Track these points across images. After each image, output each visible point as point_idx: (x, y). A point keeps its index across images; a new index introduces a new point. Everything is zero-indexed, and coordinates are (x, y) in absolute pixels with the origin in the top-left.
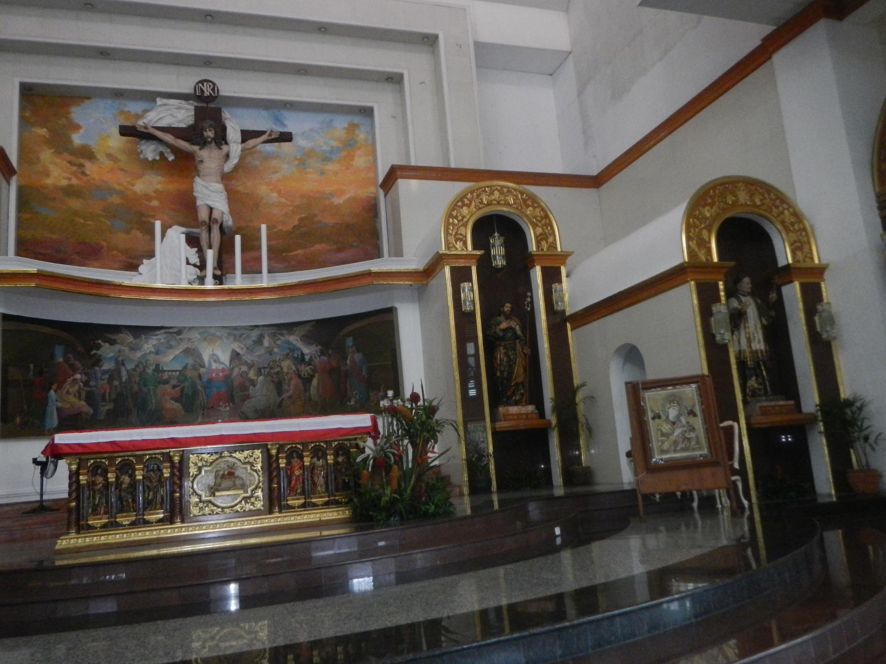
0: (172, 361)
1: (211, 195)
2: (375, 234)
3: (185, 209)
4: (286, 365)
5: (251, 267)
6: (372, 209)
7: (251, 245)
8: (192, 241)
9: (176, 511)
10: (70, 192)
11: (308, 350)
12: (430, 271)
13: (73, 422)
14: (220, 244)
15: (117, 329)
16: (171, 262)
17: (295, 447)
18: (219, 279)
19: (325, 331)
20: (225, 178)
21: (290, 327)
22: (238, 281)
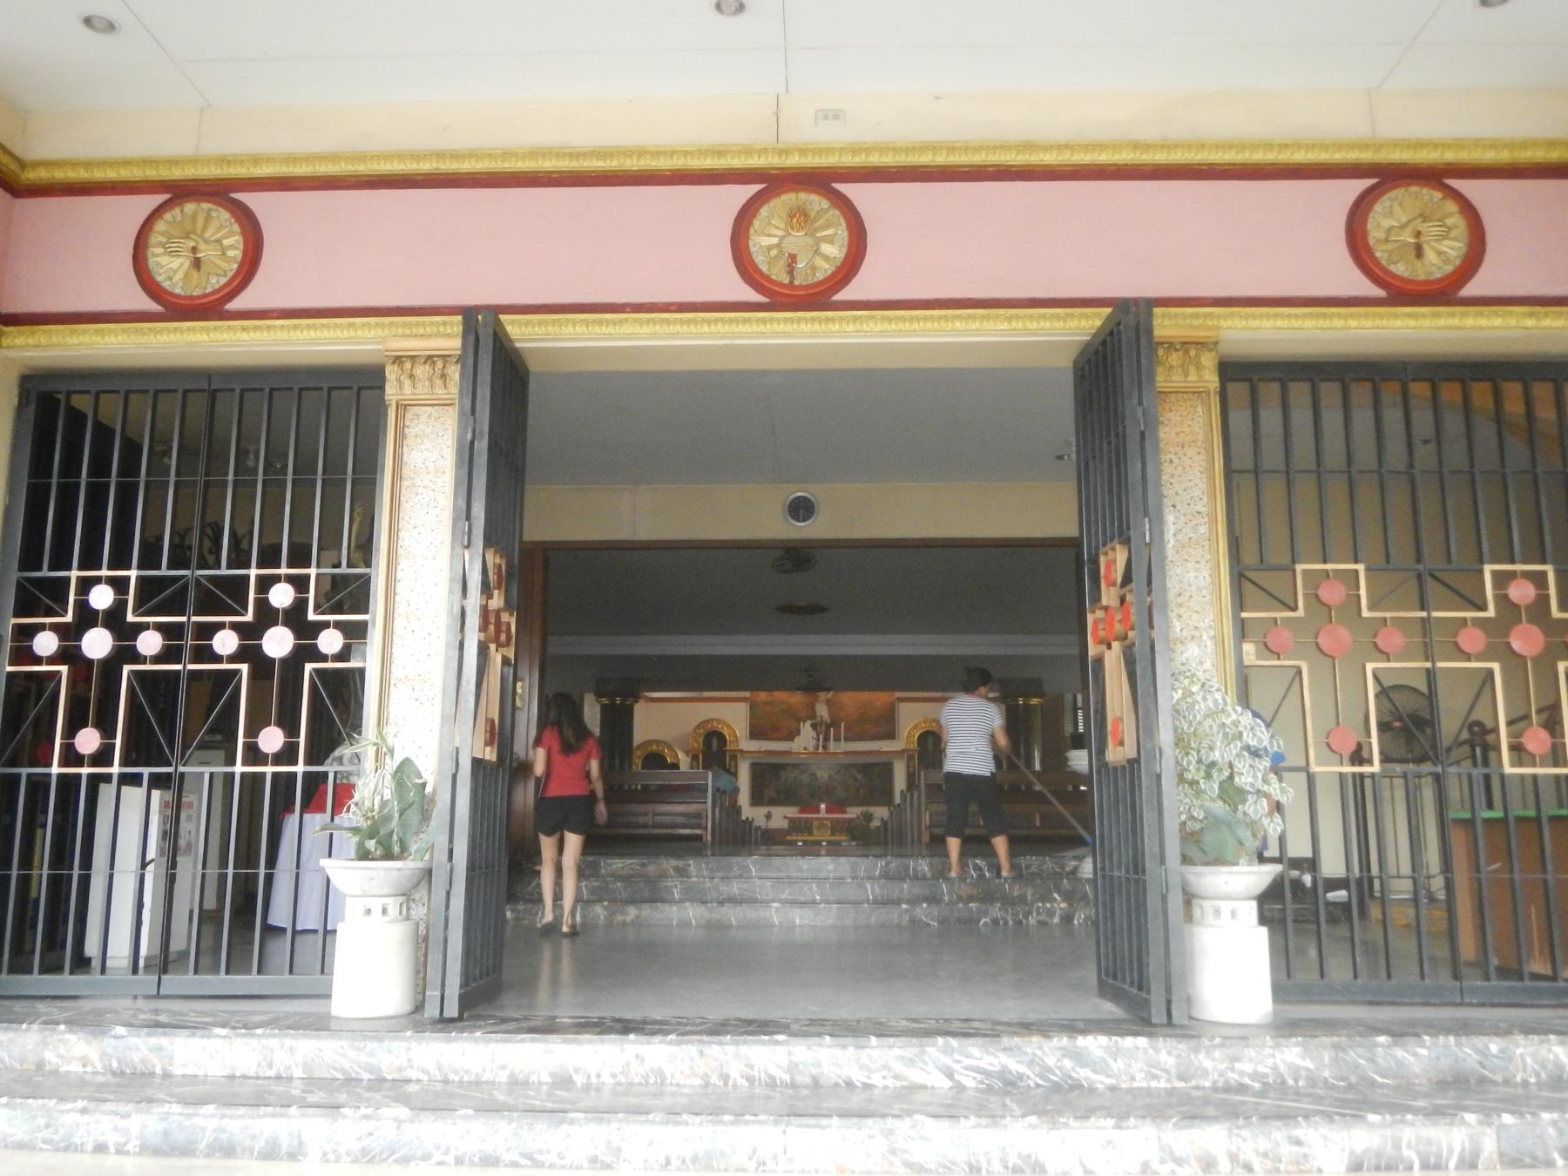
0: (805, 778)
1: (823, 711)
2: (894, 719)
3: (813, 715)
4: (851, 782)
5: (837, 739)
6: (893, 706)
7: (837, 727)
8: (814, 726)
9: (810, 833)
10: (767, 703)
11: (859, 776)
12: (903, 751)
13: (772, 802)
14: (824, 730)
15: (787, 765)
16: (806, 739)
17: (837, 821)
18: (824, 747)
19: (866, 769)
20: (828, 702)
21: (853, 766)
22: (832, 747)
